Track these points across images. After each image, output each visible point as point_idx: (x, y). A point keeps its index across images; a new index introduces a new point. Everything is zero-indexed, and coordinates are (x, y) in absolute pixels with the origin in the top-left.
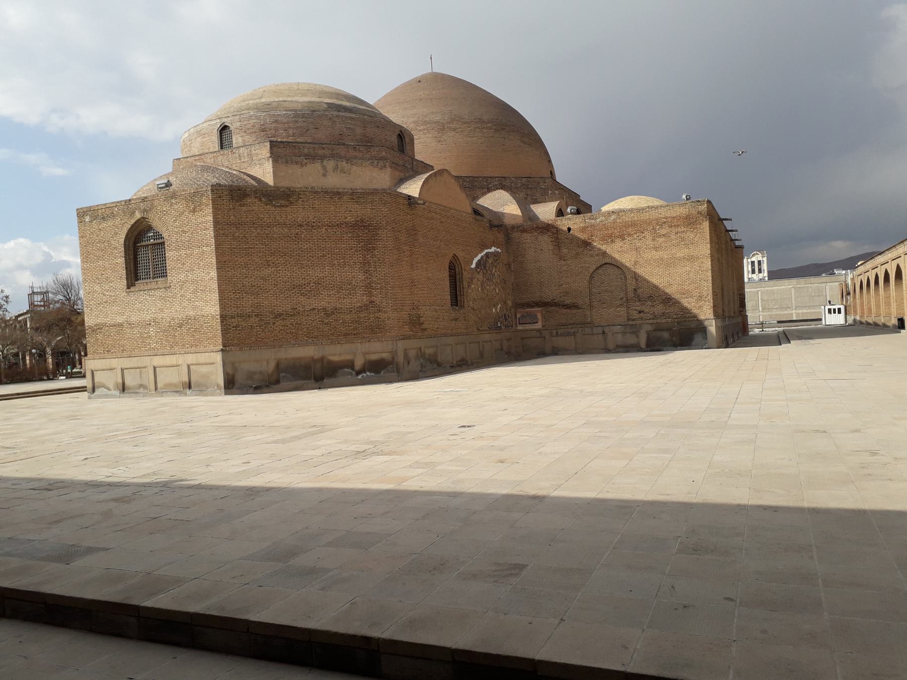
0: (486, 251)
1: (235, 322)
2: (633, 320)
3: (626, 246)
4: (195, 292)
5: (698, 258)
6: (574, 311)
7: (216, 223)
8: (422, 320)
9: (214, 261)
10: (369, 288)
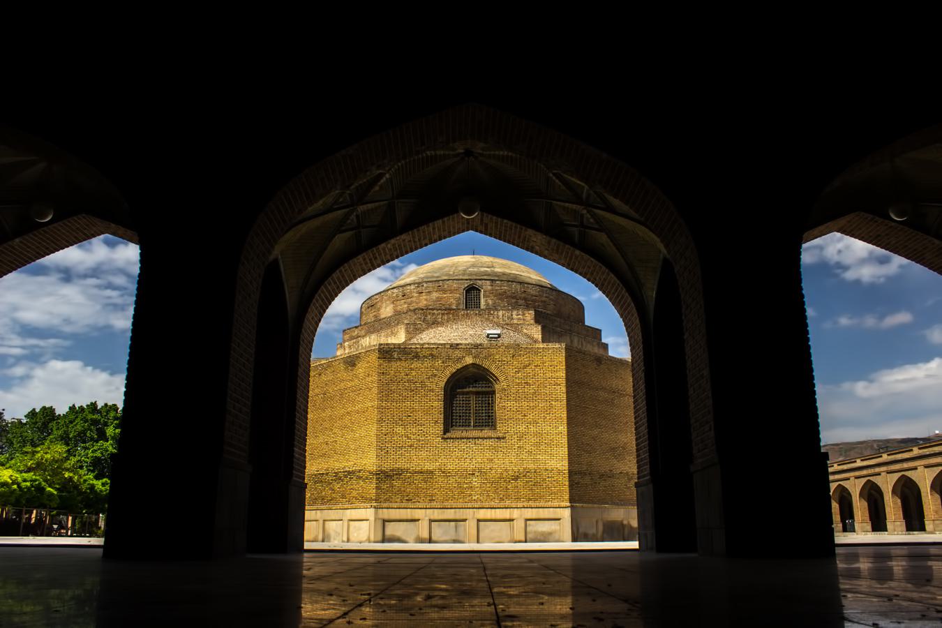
4: (538, 445)
7: (568, 380)
9: (564, 415)
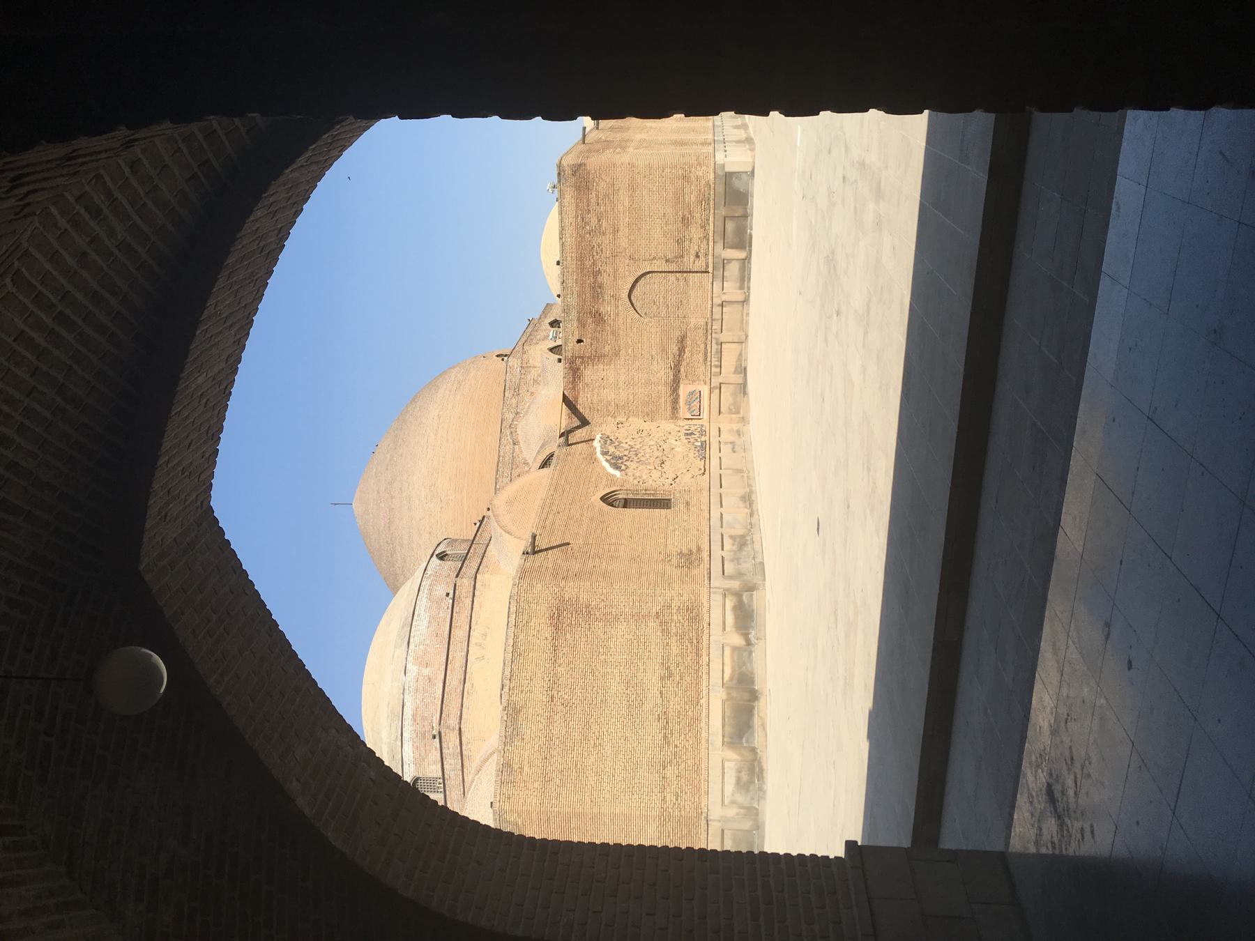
0: (599, 455)
1: (670, 798)
2: (707, 266)
3: (609, 269)
5: (633, 178)
6: (689, 343)
8: (685, 551)
10: (639, 618)
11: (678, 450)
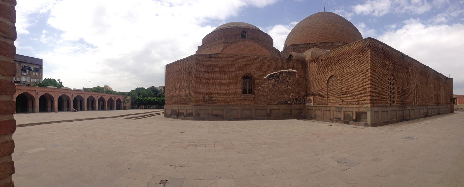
2: (340, 105)
11: (286, 96)
